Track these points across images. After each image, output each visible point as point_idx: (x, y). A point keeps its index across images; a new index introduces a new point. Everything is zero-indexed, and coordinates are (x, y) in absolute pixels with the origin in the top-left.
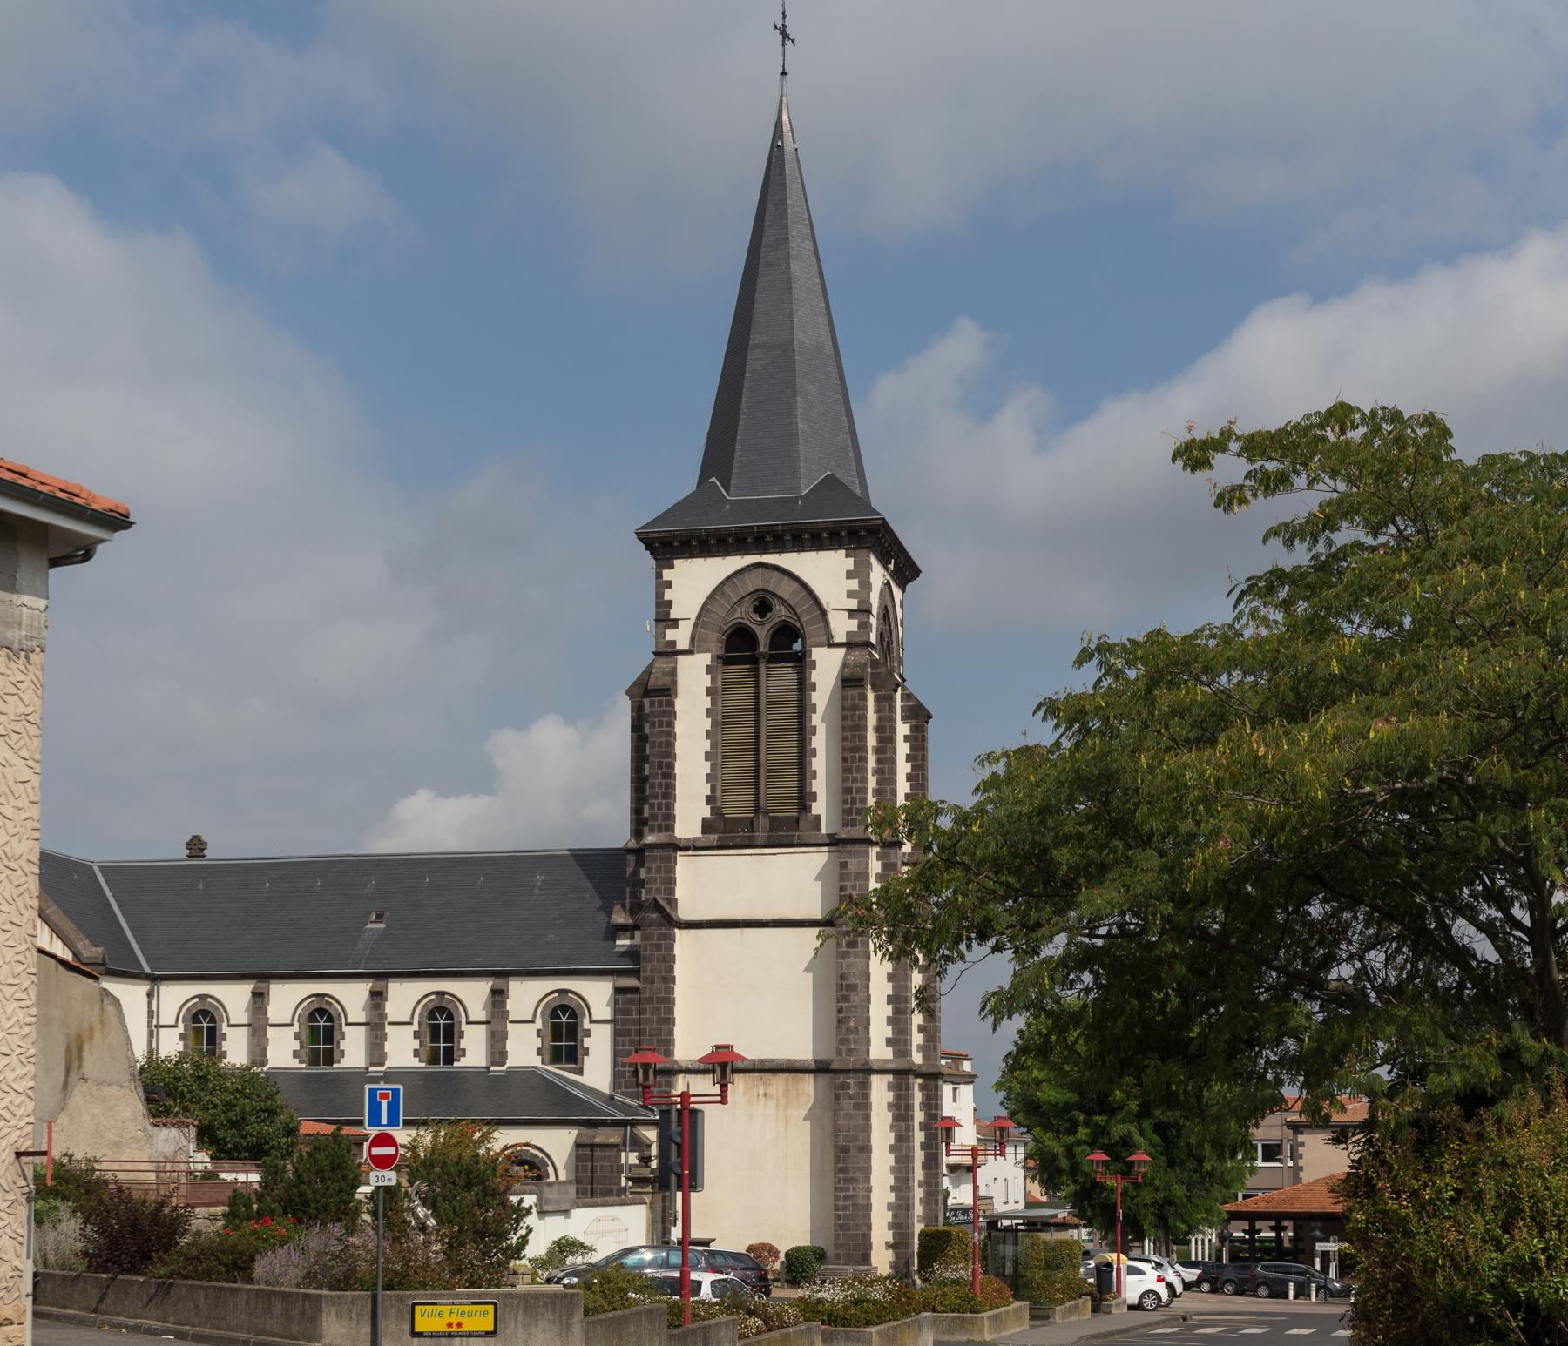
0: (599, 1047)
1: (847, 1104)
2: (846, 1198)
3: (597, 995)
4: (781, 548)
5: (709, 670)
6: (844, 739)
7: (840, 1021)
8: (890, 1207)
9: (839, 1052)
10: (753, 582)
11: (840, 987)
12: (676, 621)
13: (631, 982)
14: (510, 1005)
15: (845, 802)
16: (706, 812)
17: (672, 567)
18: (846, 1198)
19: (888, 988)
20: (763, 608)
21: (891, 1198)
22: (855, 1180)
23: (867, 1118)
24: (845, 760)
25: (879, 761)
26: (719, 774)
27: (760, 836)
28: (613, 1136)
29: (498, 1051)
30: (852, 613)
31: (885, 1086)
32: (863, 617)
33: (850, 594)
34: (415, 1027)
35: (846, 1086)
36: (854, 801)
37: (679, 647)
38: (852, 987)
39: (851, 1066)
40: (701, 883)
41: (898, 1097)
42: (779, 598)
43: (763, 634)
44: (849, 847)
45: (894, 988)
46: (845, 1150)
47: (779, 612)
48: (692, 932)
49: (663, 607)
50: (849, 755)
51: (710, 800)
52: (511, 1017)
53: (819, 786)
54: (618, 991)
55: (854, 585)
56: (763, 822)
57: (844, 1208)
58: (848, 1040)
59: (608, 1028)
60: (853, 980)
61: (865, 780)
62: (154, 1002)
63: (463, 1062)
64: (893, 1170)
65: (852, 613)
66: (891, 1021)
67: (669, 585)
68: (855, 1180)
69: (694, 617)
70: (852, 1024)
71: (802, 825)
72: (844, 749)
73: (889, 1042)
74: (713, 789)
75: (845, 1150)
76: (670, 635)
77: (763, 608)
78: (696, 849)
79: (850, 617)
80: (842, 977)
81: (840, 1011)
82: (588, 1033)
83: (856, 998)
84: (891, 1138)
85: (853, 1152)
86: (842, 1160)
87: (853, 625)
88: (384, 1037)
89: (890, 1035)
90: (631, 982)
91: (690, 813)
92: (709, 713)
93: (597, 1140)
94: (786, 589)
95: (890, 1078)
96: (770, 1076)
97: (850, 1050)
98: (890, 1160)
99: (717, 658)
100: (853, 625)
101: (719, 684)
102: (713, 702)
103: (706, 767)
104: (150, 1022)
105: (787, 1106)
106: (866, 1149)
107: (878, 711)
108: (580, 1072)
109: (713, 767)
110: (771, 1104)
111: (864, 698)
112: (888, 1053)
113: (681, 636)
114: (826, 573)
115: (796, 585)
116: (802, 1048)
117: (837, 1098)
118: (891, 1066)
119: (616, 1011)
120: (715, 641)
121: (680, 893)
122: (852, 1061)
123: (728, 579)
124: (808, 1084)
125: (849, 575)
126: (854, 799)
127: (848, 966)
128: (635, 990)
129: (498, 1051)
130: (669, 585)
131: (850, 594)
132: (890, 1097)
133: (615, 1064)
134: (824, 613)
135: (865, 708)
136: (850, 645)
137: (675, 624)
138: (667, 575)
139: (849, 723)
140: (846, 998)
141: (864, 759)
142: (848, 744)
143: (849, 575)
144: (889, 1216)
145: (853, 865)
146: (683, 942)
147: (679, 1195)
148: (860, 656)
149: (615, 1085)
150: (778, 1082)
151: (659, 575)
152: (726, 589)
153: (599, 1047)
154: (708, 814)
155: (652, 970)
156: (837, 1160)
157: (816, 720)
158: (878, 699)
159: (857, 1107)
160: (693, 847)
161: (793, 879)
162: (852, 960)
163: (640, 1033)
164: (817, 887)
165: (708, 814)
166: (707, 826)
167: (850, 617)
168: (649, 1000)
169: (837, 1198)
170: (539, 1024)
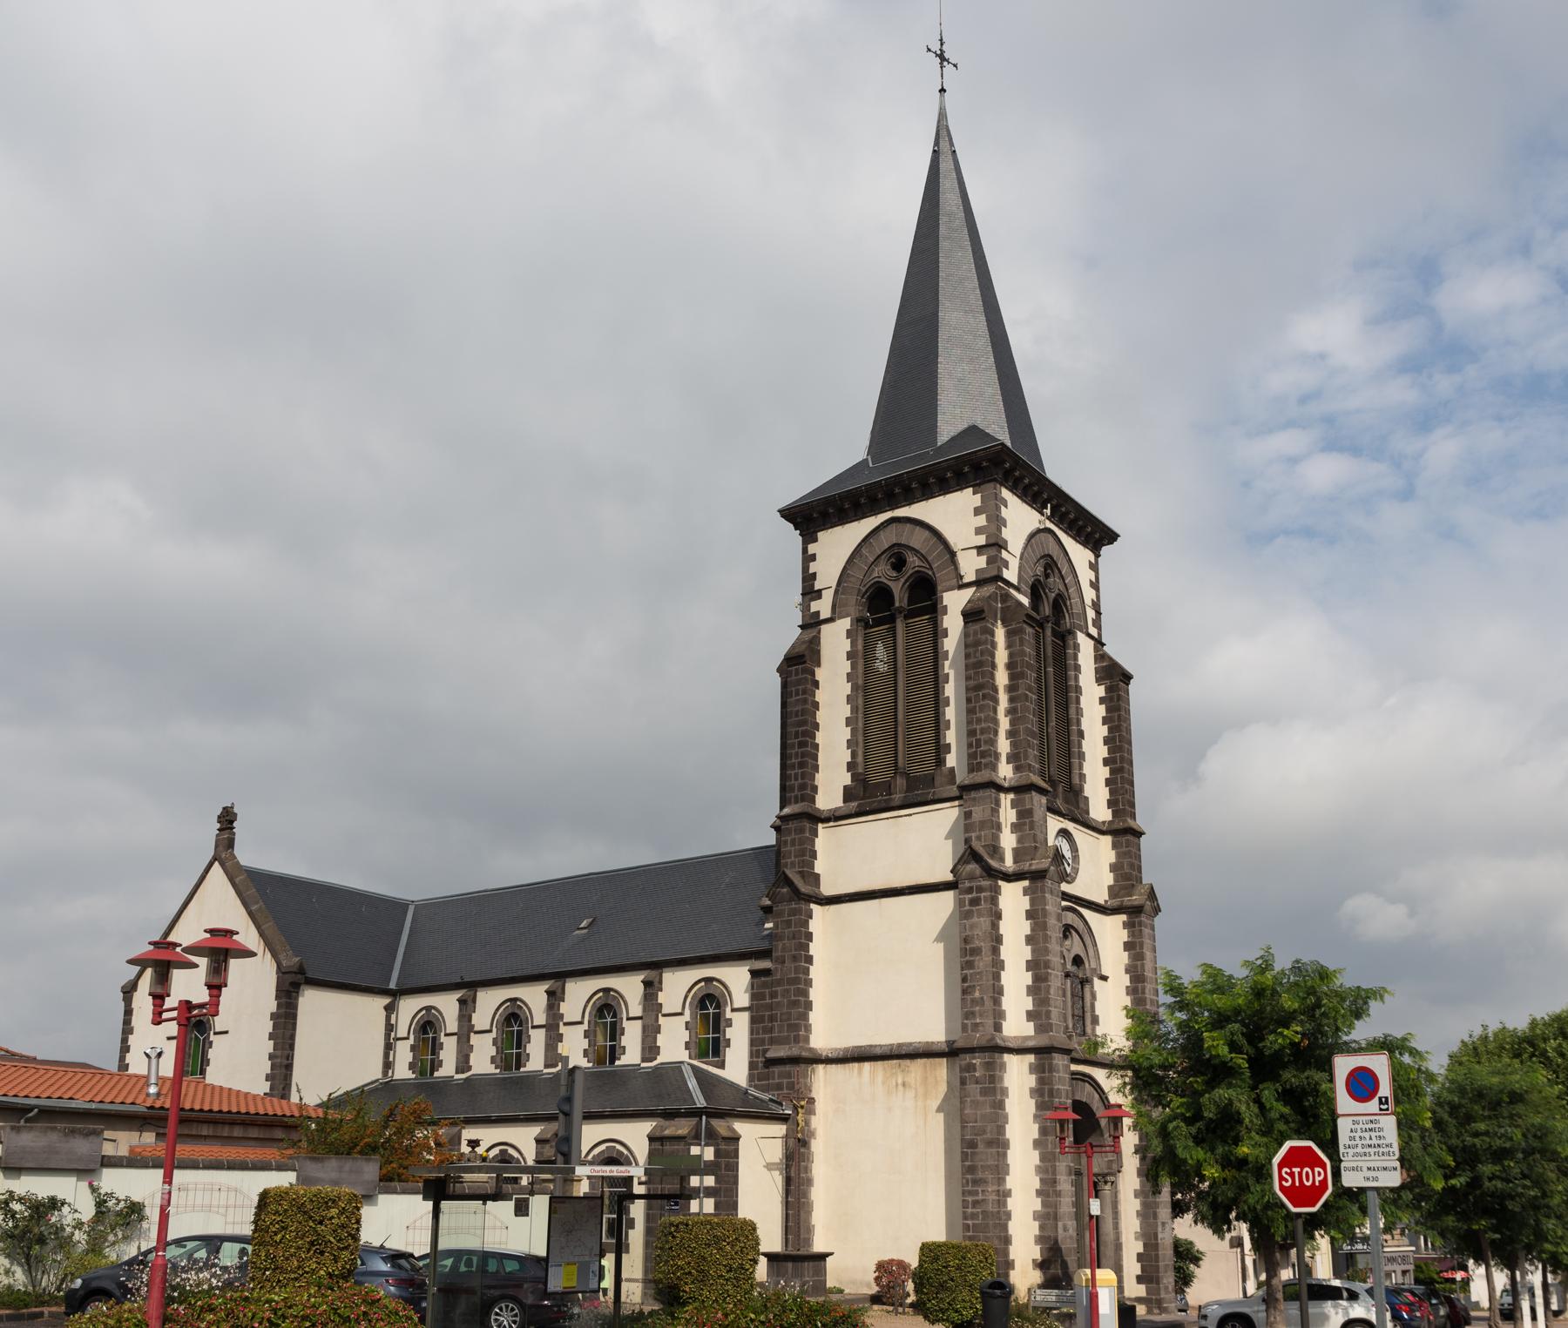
0: (739, 1032)
1: (973, 1088)
2: (975, 1203)
3: (736, 980)
4: (910, 500)
5: (849, 634)
6: (968, 678)
7: (964, 992)
9: (964, 1028)
10: (886, 539)
11: (964, 952)
12: (820, 591)
13: (764, 964)
14: (661, 998)
15: (970, 745)
16: (847, 779)
17: (816, 540)
18: (975, 1203)
19: (1027, 953)
20: (899, 564)
21: (1037, 1204)
22: (983, 1181)
23: (1000, 1105)
24: (969, 700)
25: (1011, 700)
26: (861, 739)
27: (897, 797)
28: (682, 1127)
30: (980, 549)
31: (1026, 1068)
32: (993, 551)
33: (978, 531)
34: (585, 1026)
35: (970, 1068)
36: (978, 745)
37: (822, 617)
38: (976, 951)
39: (975, 1044)
40: (841, 855)
41: (1041, 1081)
42: (912, 549)
43: (898, 589)
44: (973, 794)
45: (1033, 951)
46: (972, 1145)
47: (913, 561)
48: (833, 908)
49: (809, 578)
50: (972, 695)
51: (851, 766)
52: (665, 1011)
53: (951, 737)
54: (755, 974)
55: (982, 520)
56: (900, 782)
57: (974, 1216)
58: (973, 1013)
59: (746, 1016)
60: (977, 943)
61: (996, 722)
62: (393, 1017)
63: (623, 1061)
64: (1039, 1170)
65: (980, 549)
66: (1032, 991)
67: (813, 558)
68: (983, 1181)
69: (834, 585)
70: (977, 994)
71: (938, 780)
72: (968, 689)
73: (1030, 1016)
74: (854, 755)
75: (972, 1145)
77: (899, 564)
78: (837, 819)
79: (979, 554)
80: (966, 940)
81: (964, 980)
82: (729, 1023)
83: (982, 962)
85: (981, 1148)
86: (975, 1156)
87: (981, 562)
88: (560, 1038)
89: (1030, 1007)
90: (764, 964)
92: (850, 677)
93: (667, 1132)
94: (917, 539)
95: (1031, 1058)
96: (908, 1062)
97: (976, 1025)
98: (1035, 1157)
99: (858, 621)
100: (981, 562)
101: (860, 647)
102: (853, 666)
103: (847, 733)
104: (387, 1036)
105: (926, 1095)
106: (1000, 1144)
107: (1009, 646)
108: (722, 1065)
109: (853, 732)
110: (910, 1094)
111: (992, 634)
112: (1028, 1029)
113: (823, 607)
115: (927, 533)
116: (934, 1030)
117: (963, 1082)
118: (1031, 1044)
119: (753, 997)
120: (854, 604)
121: (819, 867)
122: (978, 1038)
123: (864, 540)
124: (941, 1069)
125: (977, 512)
126: (978, 741)
127: (972, 927)
128: (767, 972)
130: (813, 558)
131: (978, 531)
132: (1032, 1081)
133: (752, 1055)
134: (953, 554)
135: (994, 645)
136: (978, 583)
137: (818, 595)
138: (812, 548)
139: (972, 660)
140: (969, 965)
141: (996, 701)
142: (972, 683)
143: (977, 512)
145: (978, 813)
147: (467, 1177)
148: (988, 590)
149: (751, 1078)
150: (917, 1067)
151: (805, 550)
152: (864, 551)
153: (739, 1032)
154: (849, 782)
155: (784, 949)
156: (965, 1157)
157: (947, 667)
158: (1009, 634)
159: (984, 1092)
160: (835, 817)
162: (975, 919)
163: (772, 1019)
164: (948, 846)
165: (849, 782)
166: (848, 794)
167: (979, 554)
168: (779, 982)
169: (965, 1204)
170: (687, 1016)
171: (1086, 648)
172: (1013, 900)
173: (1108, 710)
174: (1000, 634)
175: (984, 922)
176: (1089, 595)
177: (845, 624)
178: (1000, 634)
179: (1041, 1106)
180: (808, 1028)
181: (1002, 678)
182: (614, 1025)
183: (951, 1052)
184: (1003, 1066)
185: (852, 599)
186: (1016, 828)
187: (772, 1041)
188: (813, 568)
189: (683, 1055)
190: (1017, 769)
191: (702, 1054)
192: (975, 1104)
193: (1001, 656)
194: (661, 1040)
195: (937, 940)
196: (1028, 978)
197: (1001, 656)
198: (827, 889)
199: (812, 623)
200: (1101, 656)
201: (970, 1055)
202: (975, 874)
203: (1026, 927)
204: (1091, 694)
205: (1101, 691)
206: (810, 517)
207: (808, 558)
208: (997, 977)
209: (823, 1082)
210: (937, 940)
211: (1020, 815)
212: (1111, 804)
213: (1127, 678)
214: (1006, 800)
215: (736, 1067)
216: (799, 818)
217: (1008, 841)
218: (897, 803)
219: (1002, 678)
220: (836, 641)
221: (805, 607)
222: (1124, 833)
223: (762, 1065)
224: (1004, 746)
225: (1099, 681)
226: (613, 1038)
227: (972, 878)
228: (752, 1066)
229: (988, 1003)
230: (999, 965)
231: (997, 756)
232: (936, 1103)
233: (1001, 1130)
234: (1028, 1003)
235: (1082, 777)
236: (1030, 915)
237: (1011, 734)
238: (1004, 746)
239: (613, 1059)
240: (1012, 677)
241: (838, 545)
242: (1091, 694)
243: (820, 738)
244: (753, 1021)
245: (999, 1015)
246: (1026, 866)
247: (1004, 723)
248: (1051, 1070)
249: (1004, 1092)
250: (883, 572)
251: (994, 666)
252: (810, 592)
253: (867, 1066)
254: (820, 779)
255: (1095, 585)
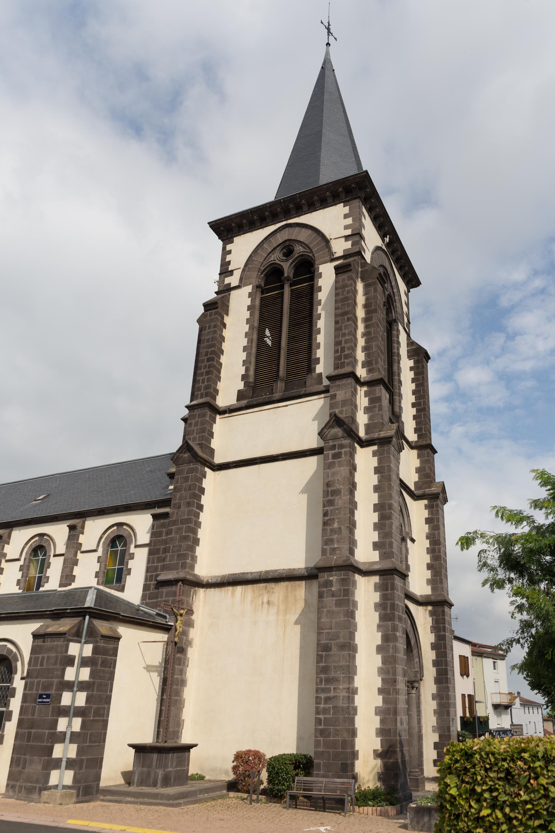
1: (330, 601)
2: (327, 700)
3: (141, 524)
4: (300, 211)
5: (250, 295)
6: (336, 309)
7: (325, 524)
8: (378, 711)
9: (324, 552)
10: (281, 238)
11: (326, 493)
12: (232, 271)
14: (82, 539)
15: (336, 351)
16: (241, 385)
18: (327, 700)
19: (375, 498)
21: (379, 701)
22: (335, 680)
23: (351, 615)
24: (336, 322)
25: (366, 327)
29: (68, 577)
30: (347, 238)
31: (372, 587)
32: (357, 238)
33: (346, 227)
35: (328, 584)
36: (343, 350)
37: (232, 286)
38: (336, 492)
39: (333, 564)
41: (384, 597)
43: (287, 268)
45: (380, 497)
47: (299, 249)
50: (339, 319)
52: (83, 549)
57: (325, 711)
58: (332, 541)
59: (146, 550)
60: (337, 486)
63: (47, 587)
64: (381, 671)
65: (347, 238)
67: (230, 252)
68: (335, 680)
69: (242, 267)
70: (336, 525)
73: (376, 546)
74: (247, 370)
76: (227, 280)
79: (346, 241)
80: (328, 485)
81: (325, 514)
82: (132, 556)
83: (341, 501)
84: (377, 638)
85: (335, 650)
86: (328, 660)
87: (348, 245)
89: (376, 539)
91: (228, 391)
94: (303, 236)
95: (376, 579)
96: (273, 585)
97: (334, 550)
98: (378, 660)
100: (348, 245)
105: (286, 611)
106: (350, 648)
107: (366, 293)
108: (122, 589)
109: (248, 355)
110: (273, 610)
114: (331, 221)
115: (310, 232)
117: (321, 596)
118: (376, 567)
120: (256, 278)
121: (215, 444)
124: (300, 590)
125: (346, 216)
127: (334, 474)
129: (68, 577)
130: (230, 252)
132: (376, 597)
137: (231, 273)
138: (229, 247)
139: (340, 297)
140: (330, 503)
142: (339, 311)
143: (346, 216)
144: (376, 722)
146: (211, 481)
149: (144, 597)
151: (224, 248)
155: (180, 498)
156: (319, 658)
157: (320, 310)
158: (366, 287)
159: (339, 604)
161: (298, 421)
162: (337, 469)
163: (166, 551)
166: (241, 395)
167: (346, 241)
168: (174, 523)
169: (318, 700)
170: (100, 553)
171: (403, 338)
172: (365, 459)
173: (415, 374)
174: (360, 286)
175: (344, 470)
176: (405, 309)
177: (248, 289)
178: (360, 286)
179: (383, 618)
180: (194, 559)
181: (360, 313)
182: (43, 561)
183: (310, 576)
184: (354, 583)
185: (255, 274)
186: (367, 410)
187: (164, 568)
188: (228, 258)
189: (93, 582)
190: (369, 371)
191: (107, 582)
192: (331, 613)
193: (361, 299)
194: (77, 571)
195: (303, 492)
196: (375, 517)
197: (361, 299)
198: (218, 459)
199: (225, 291)
200: (411, 343)
201: (327, 576)
202: (339, 432)
203: (374, 480)
204: (406, 364)
205: (411, 363)
206: (227, 229)
207: (226, 253)
208: (352, 513)
209: (203, 602)
210: (303, 492)
211: (371, 401)
212: (416, 430)
213: (427, 357)
214: (361, 391)
215: (133, 591)
216: (203, 409)
217: (362, 419)
218: (277, 396)
219: (360, 313)
220: (241, 302)
221: (221, 282)
222: (425, 449)
223: (155, 586)
224: (360, 356)
225: (409, 357)
226: (42, 571)
227: (335, 438)
228: (146, 588)
229: (345, 532)
230: (353, 506)
231: (356, 361)
232: (294, 617)
233: (352, 636)
234: (375, 537)
235: (401, 408)
236: (377, 470)
237: (365, 349)
238: (360, 356)
239: (39, 585)
240: (368, 312)
241: (245, 245)
242: (406, 364)
243: (223, 359)
244: (150, 553)
245: (353, 543)
246: (376, 435)
247: (361, 342)
248: (393, 588)
249: (355, 604)
250: (277, 257)
251: (355, 303)
252: (225, 271)
253: (239, 589)
254: (220, 386)
255: (407, 305)
